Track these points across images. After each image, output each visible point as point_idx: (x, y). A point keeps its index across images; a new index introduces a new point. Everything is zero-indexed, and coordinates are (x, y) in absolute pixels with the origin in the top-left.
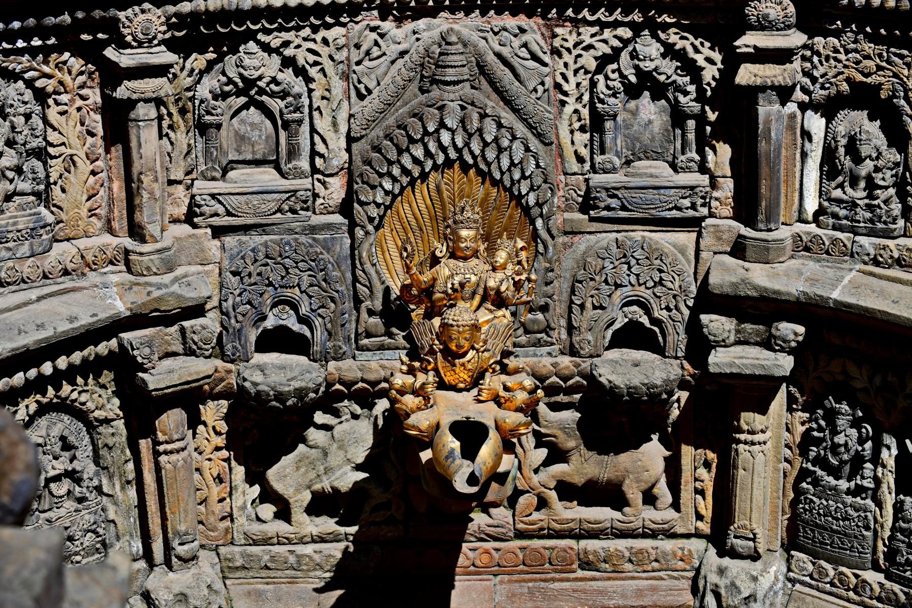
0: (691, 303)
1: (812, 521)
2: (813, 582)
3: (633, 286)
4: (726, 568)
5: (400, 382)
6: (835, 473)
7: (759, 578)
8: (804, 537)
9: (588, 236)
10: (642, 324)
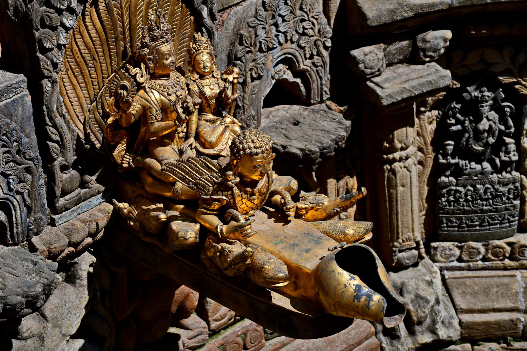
0: (329, 44)
1: (460, 210)
2: (463, 265)
3: (280, 44)
4: (403, 284)
5: (193, 235)
6: (478, 158)
7: (434, 280)
8: (448, 226)
9: (235, 8)
10: (287, 79)
